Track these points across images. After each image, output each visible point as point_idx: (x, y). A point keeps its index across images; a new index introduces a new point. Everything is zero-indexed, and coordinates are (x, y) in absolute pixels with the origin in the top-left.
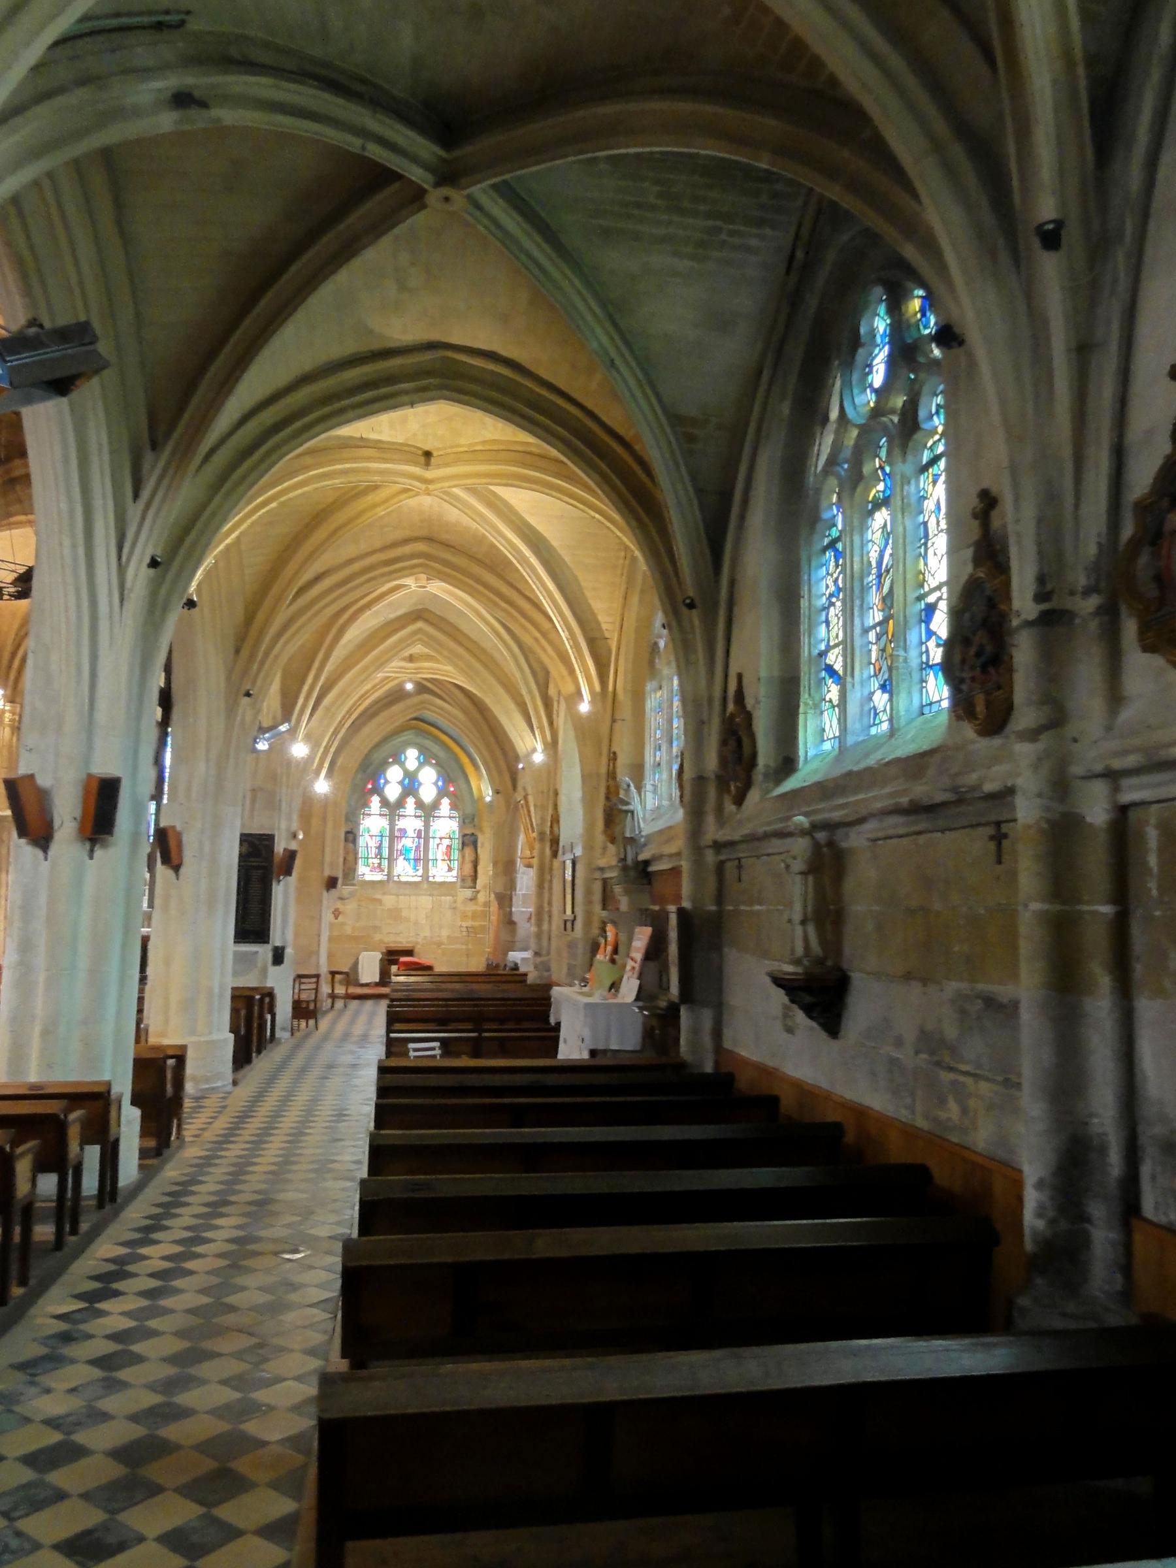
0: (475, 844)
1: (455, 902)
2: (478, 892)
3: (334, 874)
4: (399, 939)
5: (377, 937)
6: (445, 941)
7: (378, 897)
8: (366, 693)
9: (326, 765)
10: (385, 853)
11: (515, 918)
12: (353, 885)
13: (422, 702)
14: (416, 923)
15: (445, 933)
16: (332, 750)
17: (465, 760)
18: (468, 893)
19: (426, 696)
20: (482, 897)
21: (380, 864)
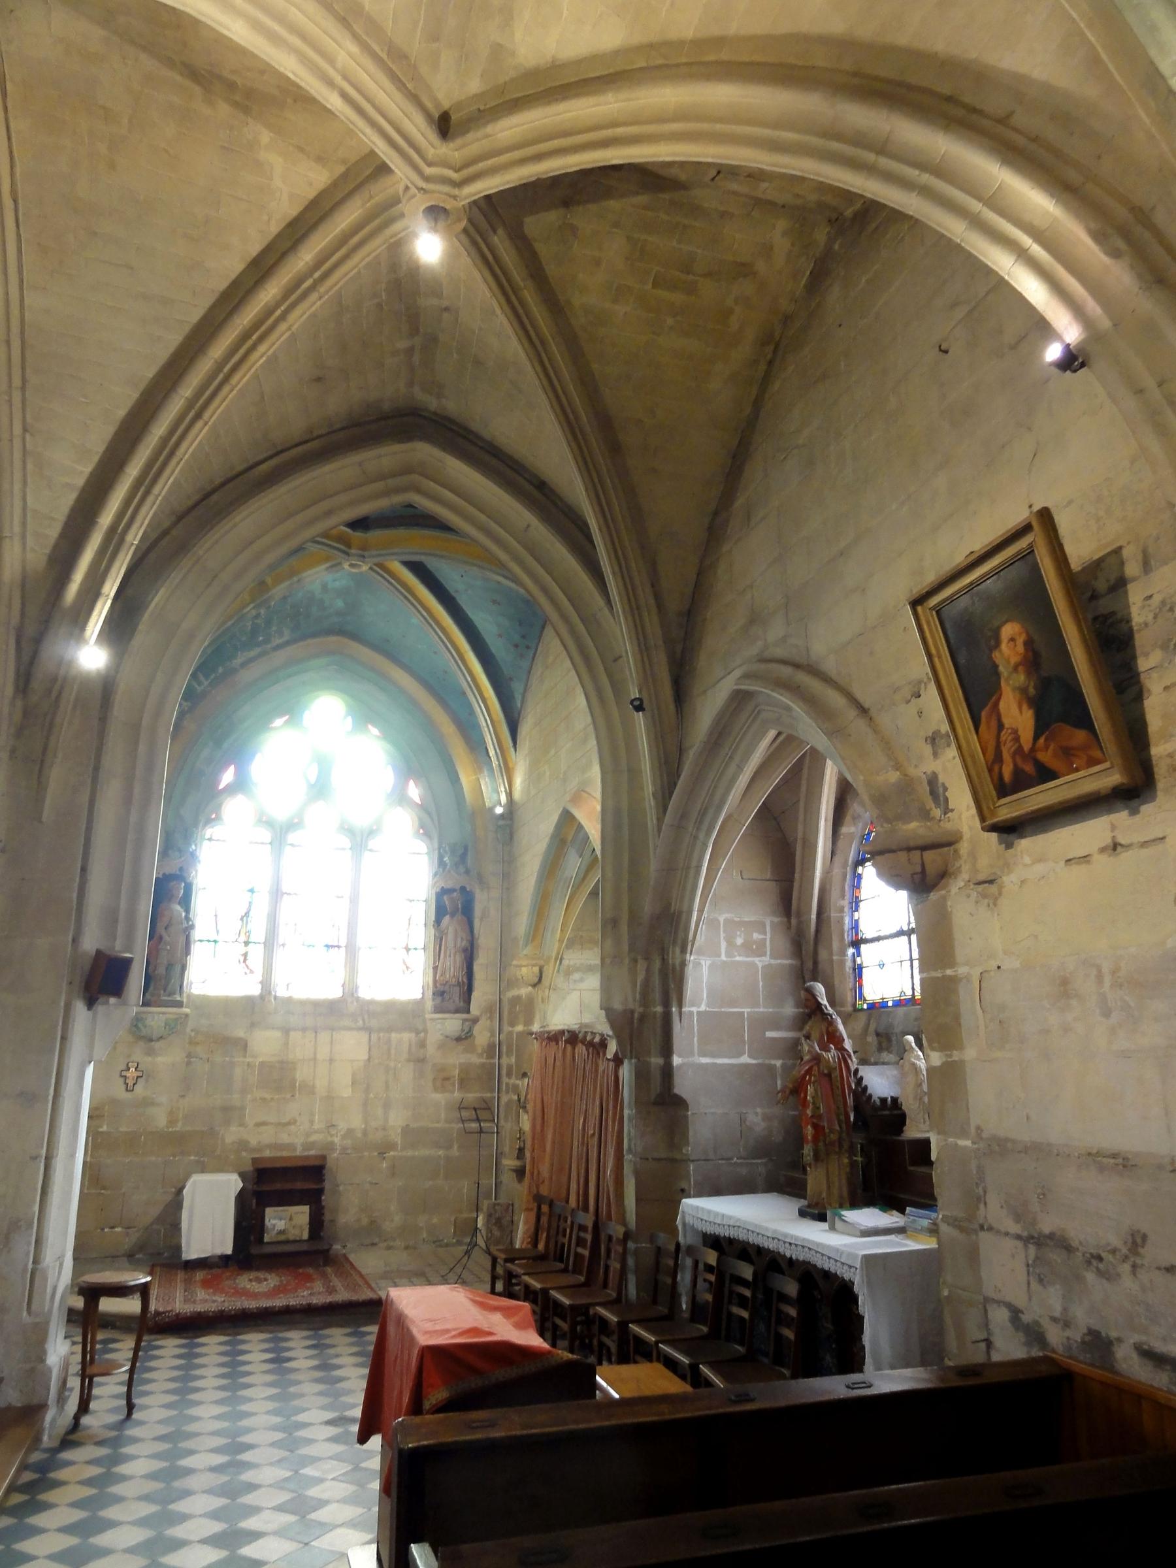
1: (422, 1045)
2: (475, 1021)
3: (119, 949)
4: (285, 1138)
5: (232, 1135)
6: (399, 1140)
7: (241, 1033)
8: (268, 312)
9: (110, 588)
10: (259, 933)
11: (683, 1087)
12: (179, 1004)
13: (407, 470)
14: (329, 1098)
15: (397, 1119)
16: (134, 537)
18: (452, 1024)
19: (424, 451)
20: (482, 1036)
21: (245, 955)
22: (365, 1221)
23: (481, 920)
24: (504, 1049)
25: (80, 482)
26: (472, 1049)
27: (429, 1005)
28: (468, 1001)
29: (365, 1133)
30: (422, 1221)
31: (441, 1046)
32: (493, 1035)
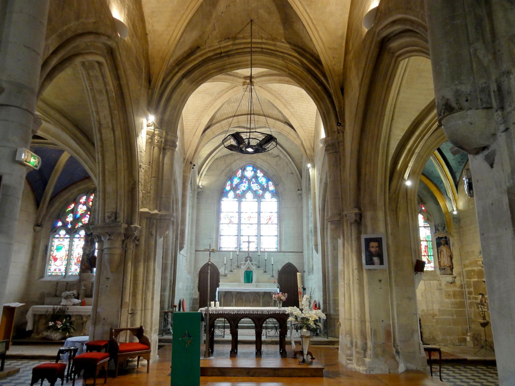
0: (447, 243)
1: (440, 285)
2: (455, 277)
17: (433, 189)
18: (449, 278)
20: (458, 282)
22: (431, 337)
23: (453, 246)
24: (466, 286)
25: (400, 138)
26: (455, 286)
27: (438, 272)
28: (452, 272)
29: (427, 311)
30: (448, 337)
31: (446, 285)
32: (461, 282)
